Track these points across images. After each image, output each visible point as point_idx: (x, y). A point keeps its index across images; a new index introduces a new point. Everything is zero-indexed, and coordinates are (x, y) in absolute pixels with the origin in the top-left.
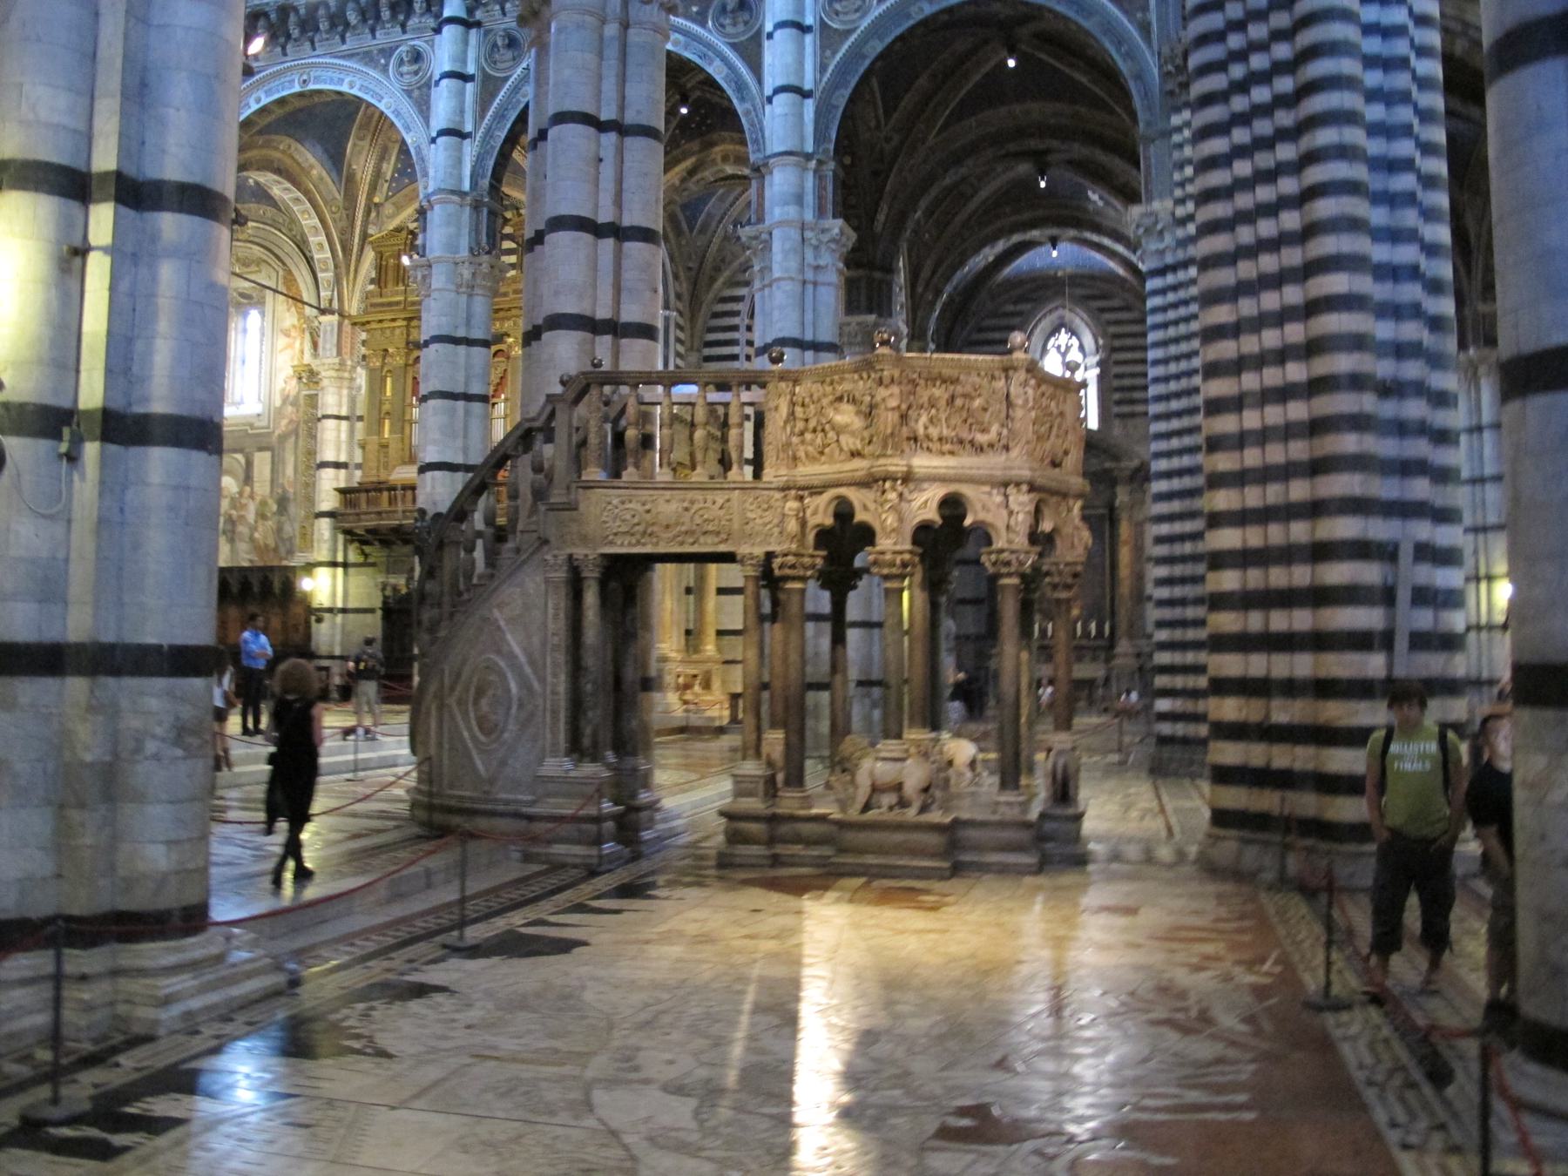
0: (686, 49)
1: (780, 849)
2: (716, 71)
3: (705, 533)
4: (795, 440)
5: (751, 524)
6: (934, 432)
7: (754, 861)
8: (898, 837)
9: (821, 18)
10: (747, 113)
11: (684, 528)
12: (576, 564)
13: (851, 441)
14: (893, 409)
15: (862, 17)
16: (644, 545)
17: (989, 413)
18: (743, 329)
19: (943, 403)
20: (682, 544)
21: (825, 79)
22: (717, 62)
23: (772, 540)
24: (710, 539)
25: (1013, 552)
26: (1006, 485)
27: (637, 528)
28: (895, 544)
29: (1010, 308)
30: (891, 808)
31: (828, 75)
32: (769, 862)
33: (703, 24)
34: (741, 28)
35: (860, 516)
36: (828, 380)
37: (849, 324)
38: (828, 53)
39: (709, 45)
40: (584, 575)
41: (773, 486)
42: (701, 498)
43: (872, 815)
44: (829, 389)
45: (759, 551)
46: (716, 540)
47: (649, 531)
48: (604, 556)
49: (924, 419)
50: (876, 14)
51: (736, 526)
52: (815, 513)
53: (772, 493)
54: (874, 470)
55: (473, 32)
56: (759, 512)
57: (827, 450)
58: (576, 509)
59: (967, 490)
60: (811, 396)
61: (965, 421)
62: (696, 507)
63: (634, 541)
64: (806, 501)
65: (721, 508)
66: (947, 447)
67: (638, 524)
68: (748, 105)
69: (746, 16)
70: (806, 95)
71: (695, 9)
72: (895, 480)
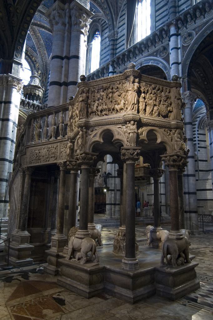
2: (160, 66)
3: (51, 157)
6: (100, 108)
8: (77, 273)
9: (182, 45)
10: (167, 73)
11: (46, 157)
15: (192, 41)
18: (196, 131)
19: (105, 97)
22: (160, 64)
24: (53, 159)
25: (127, 149)
31: (184, 57)
33: (157, 56)
34: (164, 54)
37: (211, 122)
38: (184, 52)
39: (158, 61)
42: (51, 146)
50: (195, 38)
61: (112, 102)
67: (37, 157)
68: (167, 71)
69: (166, 51)
71: (155, 54)
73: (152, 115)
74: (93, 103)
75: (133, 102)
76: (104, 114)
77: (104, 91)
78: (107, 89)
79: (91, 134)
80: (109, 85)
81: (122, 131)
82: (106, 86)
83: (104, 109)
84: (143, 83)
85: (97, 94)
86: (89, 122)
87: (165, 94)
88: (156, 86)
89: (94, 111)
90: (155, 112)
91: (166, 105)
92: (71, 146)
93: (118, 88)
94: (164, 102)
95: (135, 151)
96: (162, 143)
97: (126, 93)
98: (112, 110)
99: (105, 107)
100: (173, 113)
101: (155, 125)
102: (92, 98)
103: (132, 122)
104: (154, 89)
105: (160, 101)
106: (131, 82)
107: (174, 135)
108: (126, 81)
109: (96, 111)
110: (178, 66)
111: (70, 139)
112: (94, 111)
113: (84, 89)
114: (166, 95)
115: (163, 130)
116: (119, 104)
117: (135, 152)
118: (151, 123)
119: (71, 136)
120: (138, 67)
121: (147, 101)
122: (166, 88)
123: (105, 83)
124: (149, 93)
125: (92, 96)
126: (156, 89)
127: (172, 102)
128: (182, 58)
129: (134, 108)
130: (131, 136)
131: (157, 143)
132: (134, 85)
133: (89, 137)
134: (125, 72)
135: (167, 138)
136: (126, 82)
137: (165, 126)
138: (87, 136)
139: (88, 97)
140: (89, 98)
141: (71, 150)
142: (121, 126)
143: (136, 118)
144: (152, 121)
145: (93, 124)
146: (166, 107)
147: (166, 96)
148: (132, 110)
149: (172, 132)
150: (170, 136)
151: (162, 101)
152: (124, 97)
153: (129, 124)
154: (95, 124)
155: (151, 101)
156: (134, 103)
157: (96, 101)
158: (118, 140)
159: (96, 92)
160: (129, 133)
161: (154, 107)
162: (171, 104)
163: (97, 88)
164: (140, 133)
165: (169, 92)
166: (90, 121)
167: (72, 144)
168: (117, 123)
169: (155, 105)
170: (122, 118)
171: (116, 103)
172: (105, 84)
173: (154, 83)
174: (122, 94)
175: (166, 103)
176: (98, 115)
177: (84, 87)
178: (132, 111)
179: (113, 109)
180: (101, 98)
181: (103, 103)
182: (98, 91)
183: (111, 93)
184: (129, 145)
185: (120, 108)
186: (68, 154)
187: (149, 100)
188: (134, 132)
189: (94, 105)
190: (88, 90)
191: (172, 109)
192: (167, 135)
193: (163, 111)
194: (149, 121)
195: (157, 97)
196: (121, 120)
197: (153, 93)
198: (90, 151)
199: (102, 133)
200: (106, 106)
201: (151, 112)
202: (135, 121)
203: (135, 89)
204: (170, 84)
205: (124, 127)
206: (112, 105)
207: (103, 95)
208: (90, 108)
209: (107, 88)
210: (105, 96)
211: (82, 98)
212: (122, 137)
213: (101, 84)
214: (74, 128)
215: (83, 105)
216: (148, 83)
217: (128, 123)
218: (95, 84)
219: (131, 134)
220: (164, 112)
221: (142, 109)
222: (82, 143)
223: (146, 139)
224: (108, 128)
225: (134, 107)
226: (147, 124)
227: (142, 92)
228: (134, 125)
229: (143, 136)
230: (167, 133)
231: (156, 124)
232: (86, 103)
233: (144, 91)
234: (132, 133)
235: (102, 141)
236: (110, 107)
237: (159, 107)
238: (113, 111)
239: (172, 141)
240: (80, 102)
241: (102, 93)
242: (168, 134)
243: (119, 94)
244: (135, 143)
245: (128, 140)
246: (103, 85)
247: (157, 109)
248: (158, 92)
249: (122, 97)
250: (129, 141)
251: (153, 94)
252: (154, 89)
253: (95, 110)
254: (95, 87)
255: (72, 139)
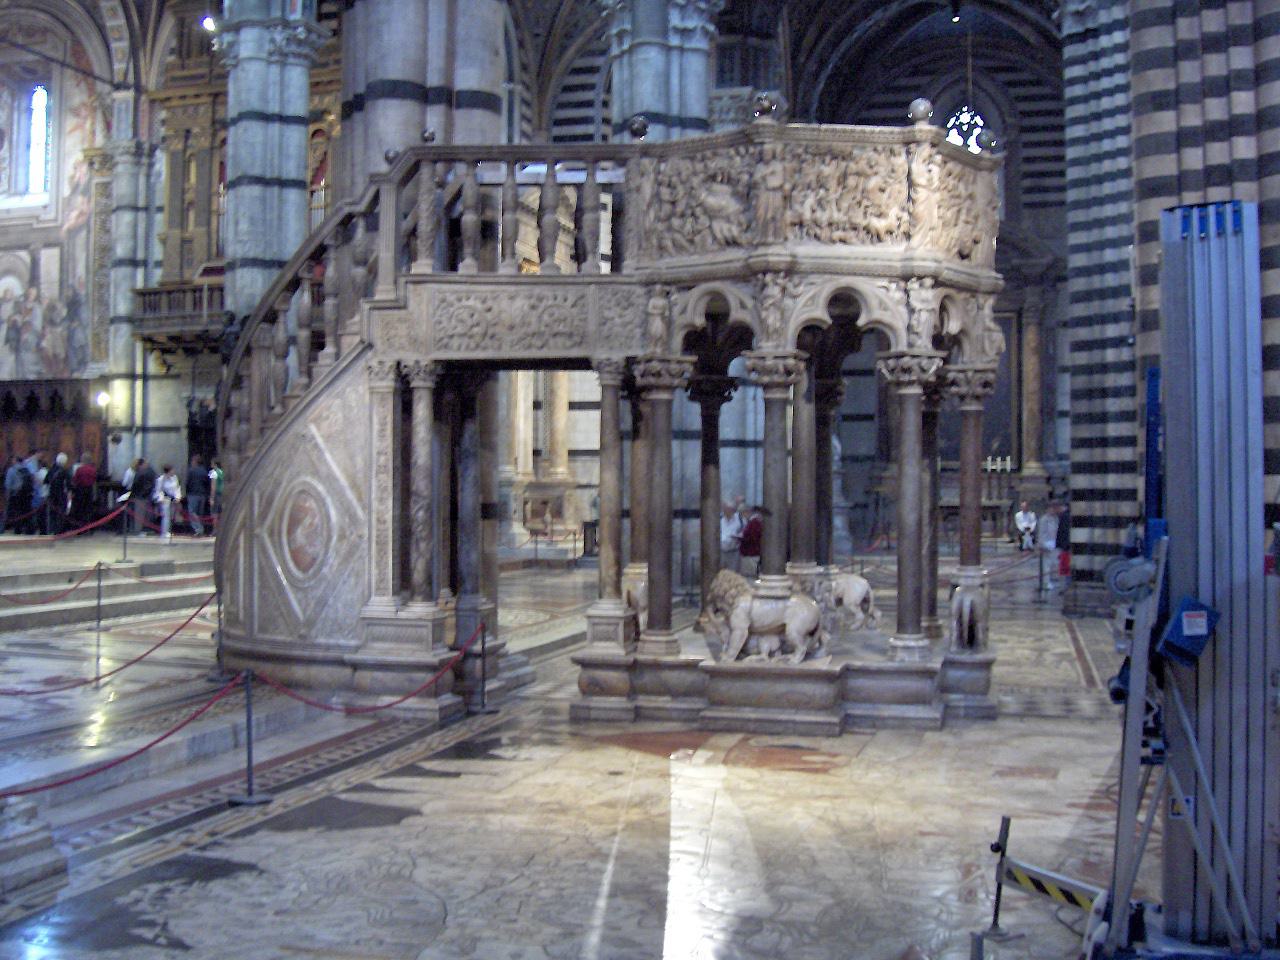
1: (643, 701)
3: (555, 335)
4: (660, 226)
5: (609, 324)
7: (612, 715)
8: (781, 687)
12: (404, 371)
13: (725, 226)
14: (774, 189)
16: (485, 348)
20: (530, 347)
23: (634, 342)
25: (914, 356)
26: (906, 278)
27: (476, 330)
29: (903, 82)
30: (771, 654)
32: (631, 716)
35: (737, 315)
36: (699, 156)
37: (720, 98)
40: (413, 385)
41: (634, 280)
43: (750, 662)
44: (699, 166)
45: (618, 356)
46: (569, 343)
47: (490, 332)
48: (437, 362)
49: (811, 201)
51: (592, 327)
52: (684, 311)
53: (633, 288)
54: (752, 260)
56: (618, 310)
57: (697, 239)
58: (405, 307)
59: (862, 284)
60: (679, 174)
62: (544, 303)
63: (473, 345)
64: (673, 298)
65: (573, 306)
66: (838, 234)
67: (478, 324)
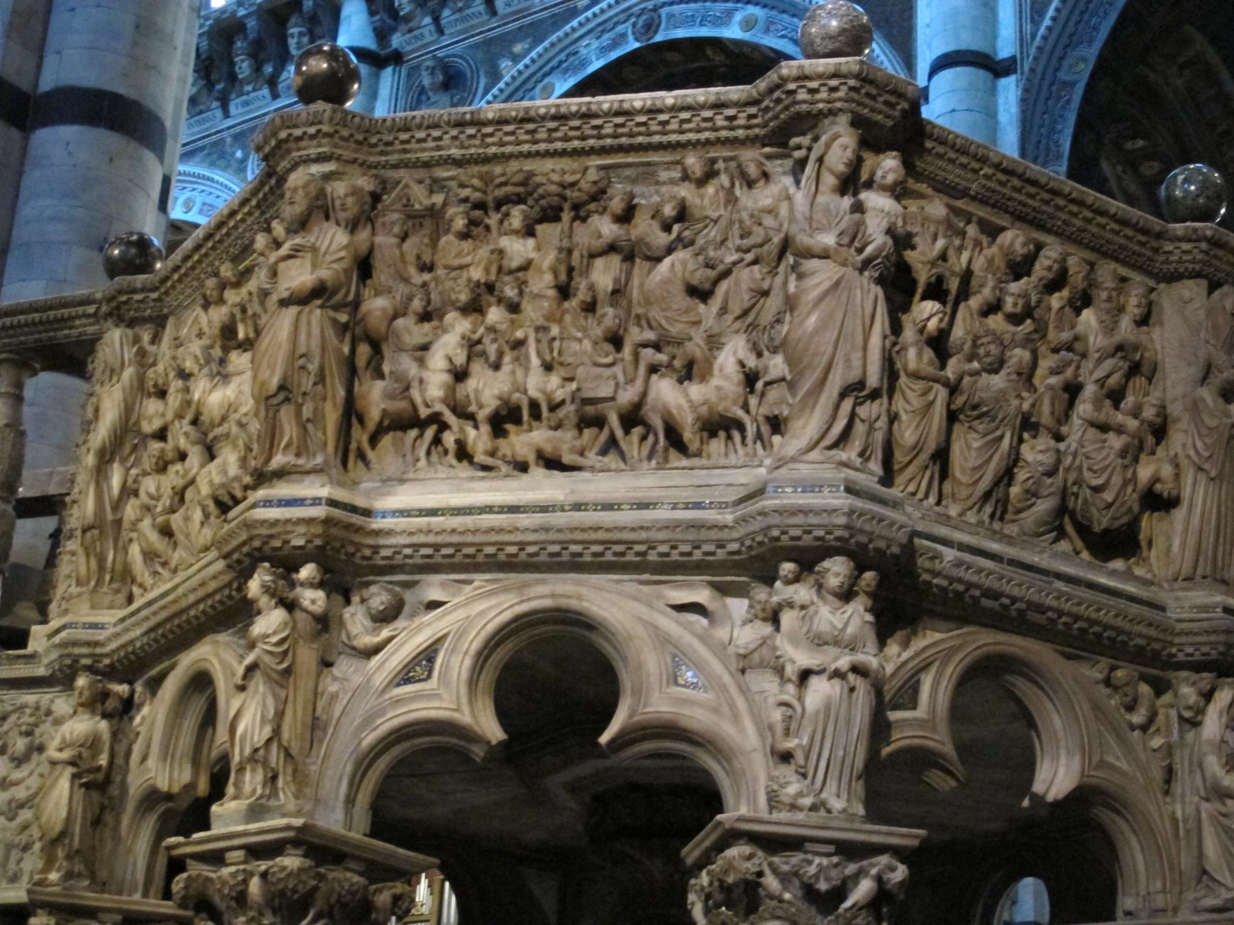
0: (767, 31)
17: (715, 303)
19: (542, 283)
21: (1042, 30)
25: (774, 844)
28: (256, 811)
31: (1047, 22)
55: (387, 74)
61: (616, 340)
70: (997, 68)
72: (287, 564)
73: (1002, 512)
74: (411, 331)
75: (854, 376)
76: (531, 458)
77: (540, 228)
78: (566, 216)
79: (368, 640)
80: (593, 175)
81: (720, 649)
82: (563, 186)
83: (534, 406)
84: (921, 196)
85: (466, 245)
86: (367, 513)
87: (1110, 328)
88: (1039, 247)
89: (424, 412)
90: (1032, 494)
91: (1120, 430)
92: (93, 744)
93: (683, 215)
94: (1108, 402)
95: (851, 868)
96: (1082, 796)
97: (773, 272)
98: (614, 420)
99: (538, 384)
100: (1179, 514)
101: (1033, 616)
102: (406, 280)
103: (836, 569)
104: (1019, 268)
105: (1073, 390)
106: (829, 180)
107: (1190, 736)
108: (769, 157)
109: (450, 418)
110: (993, 90)
111: (90, 669)
112: (424, 412)
113: (327, 177)
114: (1117, 339)
115: (1093, 672)
116: (688, 372)
117: (857, 877)
118: (995, 595)
119: (101, 635)
120: (615, 44)
121: (967, 379)
122: (1124, 280)
123: (563, 153)
124: (975, 302)
125: (411, 258)
126: (1041, 269)
127: (1175, 409)
128: (1028, 28)
129: (860, 428)
130: (828, 708)
131: (1038, 800)
132: (858, 208)
133: (345, 667)
134: (784, 80)
135: (1129, 751)
136: (774, 167)
137: (1119, 631)
138: (329, 665)
139: (364, 267)
140: (382, 275)
141: (87, 786)
142: (702, 595)
143: (878, 529)
144: (1008, 571)
145: (416, 547)
146: (1123, 453)
147: (1120, 348)
148: (835, 445)
149: (1167, 698)
150: (1157, 742)
151: (1090, 390)
152: (746, 313)
153: (797, 579)
154: (437, 547)
155: (998, 381)
156: (861, 385)
157: (451, 316)
158: (671, 730)
159: (460, 223)
160: (805, 675)
161: (1021, 441)
162: (1160, 431)
163: (465, 193)
164: (896, 683)
165: (1143, 321)
166: (381, 504)
167: (103, 725)
168: (675, 556)
169: (1028, 425)
170: (728, 518)
171: (662, 358)
172: (549, 164)
173: (1021, 218)
174: (726, 274)
175: (1120, 418)
176: (463, 454)
177: (338, 159)
178: (842, 455)
179: (633, 418)
180: (510, 292)
181: (519, 344)
182: (473, 223)
183: (615, 260)
184: (807, 801)
185: (704, 410)
186: (58, 828)
187: (976, 365)
188: (856, 669)
189: (425, 348)
190: (376, 198)
191: (1177, 476)
192: (1133, 728)
193: (1097, 490)
194: (984, 573)
195: (1043, 349)
196: (714, 535)
197: (1009, 301)
198: (349, 826)
199: (497, 645)
200: (554, 380)
201: (996, 484)
202: (861, 559)
203: (869, 250)
204: (1155, 244)
205: (738, 606)
206: (618, 370)
207: (526, 267)
208: (381, 376)
209: (576, 207)
210: (548, 278)
211: (314, 266)
212: (716, 711)
213: (511, 156)
214: (150, 555)
215: (315, 344)
216: (972, 208)
217: (788, 568)
218: (455, 152)
219: (820, 690)
220: (1108, 496)
221: (917, 449)
222: (277, 732)
223: (948, 749)
224: (574, 604)
225: (853, 416)
226: (959, 595)
227: (914, 282)
228: (846, 595)
229: (921, 712)
230: (1130, 708)
231: (1040, 608)
232: (343, 318)
233: (940, 279)
234: (837, 674)
235: (494, 731)
236: (605, 391)
237: (1062, 446)
238: (627, 429)
239: (1177, 788)
240: (284, 303)
241: (518, 249)
242: (1137, 718)
243: (700, 276)
244: (859, 787)
245: (791, 744)
246: (529, 166)
247: (1048, 459)
248: (1056, 301)
249: (724, 310)
250: (800, 758)
251: (1015, 319)
252: (1019, 268)
253: (439, 407)
254: (442, 173)
255: (111, 673)
